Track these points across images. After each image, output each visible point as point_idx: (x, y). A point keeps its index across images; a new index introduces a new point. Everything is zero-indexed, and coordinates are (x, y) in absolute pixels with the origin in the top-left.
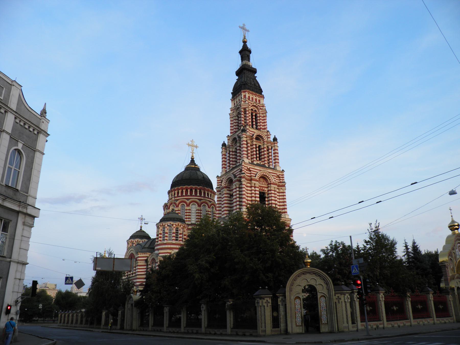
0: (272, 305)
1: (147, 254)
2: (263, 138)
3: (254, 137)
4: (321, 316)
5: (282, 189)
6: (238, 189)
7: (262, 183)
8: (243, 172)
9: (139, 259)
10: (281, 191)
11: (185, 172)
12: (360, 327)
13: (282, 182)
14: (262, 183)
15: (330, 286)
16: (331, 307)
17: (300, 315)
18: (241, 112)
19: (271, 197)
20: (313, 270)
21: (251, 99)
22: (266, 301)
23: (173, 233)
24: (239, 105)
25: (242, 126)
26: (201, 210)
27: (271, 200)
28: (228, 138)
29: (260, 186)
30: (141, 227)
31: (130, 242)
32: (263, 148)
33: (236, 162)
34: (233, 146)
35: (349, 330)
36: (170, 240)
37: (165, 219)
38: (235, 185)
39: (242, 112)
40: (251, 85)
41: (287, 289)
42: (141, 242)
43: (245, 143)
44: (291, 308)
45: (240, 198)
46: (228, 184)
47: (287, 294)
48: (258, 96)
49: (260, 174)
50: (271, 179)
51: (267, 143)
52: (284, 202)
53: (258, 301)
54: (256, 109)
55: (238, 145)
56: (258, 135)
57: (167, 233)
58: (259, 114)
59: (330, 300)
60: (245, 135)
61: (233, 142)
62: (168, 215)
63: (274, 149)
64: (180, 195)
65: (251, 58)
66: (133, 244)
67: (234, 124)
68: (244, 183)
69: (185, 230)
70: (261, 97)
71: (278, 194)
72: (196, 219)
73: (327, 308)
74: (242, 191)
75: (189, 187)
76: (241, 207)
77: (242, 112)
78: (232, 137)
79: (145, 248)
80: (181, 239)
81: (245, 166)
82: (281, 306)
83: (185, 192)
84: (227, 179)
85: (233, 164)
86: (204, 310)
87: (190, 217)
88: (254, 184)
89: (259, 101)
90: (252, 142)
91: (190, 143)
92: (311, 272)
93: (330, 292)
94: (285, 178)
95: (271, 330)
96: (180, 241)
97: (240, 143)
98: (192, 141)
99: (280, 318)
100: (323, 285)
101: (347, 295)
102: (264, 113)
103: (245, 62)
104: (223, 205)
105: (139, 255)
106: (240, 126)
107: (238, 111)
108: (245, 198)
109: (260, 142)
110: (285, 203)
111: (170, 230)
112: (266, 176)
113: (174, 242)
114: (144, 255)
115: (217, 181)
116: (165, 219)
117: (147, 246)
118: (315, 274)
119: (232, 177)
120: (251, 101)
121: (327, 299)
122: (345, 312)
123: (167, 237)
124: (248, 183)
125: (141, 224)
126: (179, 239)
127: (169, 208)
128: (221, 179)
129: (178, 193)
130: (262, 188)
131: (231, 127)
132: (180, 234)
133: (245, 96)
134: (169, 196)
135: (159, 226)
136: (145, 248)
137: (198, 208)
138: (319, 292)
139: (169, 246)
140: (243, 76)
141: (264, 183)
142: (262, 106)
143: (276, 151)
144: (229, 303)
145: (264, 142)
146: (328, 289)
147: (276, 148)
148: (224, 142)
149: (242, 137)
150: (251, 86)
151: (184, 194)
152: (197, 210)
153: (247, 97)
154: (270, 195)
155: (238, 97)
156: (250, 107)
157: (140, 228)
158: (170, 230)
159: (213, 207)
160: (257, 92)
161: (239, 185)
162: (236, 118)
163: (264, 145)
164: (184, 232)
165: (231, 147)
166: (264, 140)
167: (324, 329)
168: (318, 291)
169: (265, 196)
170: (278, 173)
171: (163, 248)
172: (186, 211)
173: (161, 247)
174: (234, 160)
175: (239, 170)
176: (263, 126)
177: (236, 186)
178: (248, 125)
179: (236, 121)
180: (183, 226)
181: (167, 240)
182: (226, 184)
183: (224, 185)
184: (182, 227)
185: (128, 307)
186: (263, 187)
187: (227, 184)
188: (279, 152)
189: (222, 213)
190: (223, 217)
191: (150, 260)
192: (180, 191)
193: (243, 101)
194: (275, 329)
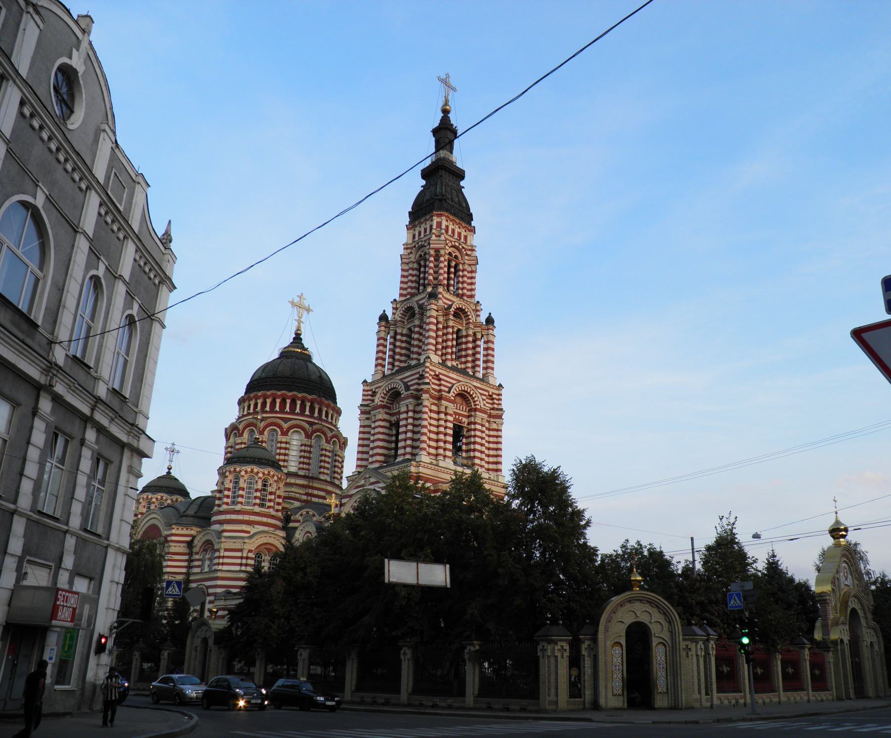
0: (569, 657)
1: (192, 529)
2: (468, 316)
3: (451, 310)
4: (657, 679)
5: (495, 422)
6: (410, 414)
8: (427, 381)
9: (174, 538)
10: (494, 426)
11: (281, 362)
12: (716, 702)
13: (498, 409)
15: (674, 626)
16: (675, 664)
17: (620, 676)
18: (427, 256)
19: (475, 436)
20: (647, 596)
21: (450, 233)
22: (560, 648)
23: (257, 490)
24: (425, 241)
25: (429, 284)
26: (310, 446)
27: (475, 443)
28: (395, 306)
29: (456, 413)
30: (169, 469)
31: (143, 498)
32: (467, 336)
33: (408, 356)
34: (404, 322)
35: (701, 705)
36: (248, 504)
37: (241, 459)
38: (405, 405)
39: (431, 256)
40: (453, 204)
41: (601, 628)
42: (169, 501)
43: (435, 321)
44: (606, 662)
45: (414, 432)
46: (388, 401)
47: (601, 636)
48: (463, 228)
49: (458, 388)
50: (477, 401)
51: (475, 327)
52: (497, 449)
53: (543, 646)
54: (458, 254)
55: (417, 322)
56: (458, 309)
57: (243, 489)
59: (674, 652)
60: (435, 305)
61: (406, 316)
62: (247, 451)
63: (486, 340)
64: (268, 409)
65: (455, 147)
66: (150, 503)
67: (410, 278)
68: (426, 403)
69: (281, 485)
70: (470, 231)
71: (487, 432)
72: (298, 463)
73: (668, 665)
74: (420, 419)
75: (290, 394)
76: (415, 451)
77: (431, 256)
78: (404, 304)
79: (187, 516)
80: (272, 504)
81: (431, 370)
82: (586, 658)
83: (280, 403)
84: (387, 390)
85: (401, 361)
86: (408, 659)
87: (286, 458)
88: (444, 407)
89: (466, 237)
90: (447, 320)
91: (297, 300)
92: (644, 599)
93: (674, 637)
94: (502, 402)
95: (567, 701)
96: (269, 507)
97: (421, 320)
98: (300, 297)
99: (584, 681)
100: (663, 623)
101: (701, 643)
102: (473, 265)
103: (443, 153)
104: (373, 441)
105: (174, 531)
106: (425, 286)
107: (419, 253)
108: (425, 434)
109: (460, 323)
110: (499, 453)
111: (250, 483)
112: (469, 393)
113: (257, 509)
114: (185, 532)
115: (364, 390)
116: (241, 457)
117: (191, 512)
118: (650, 603)
119: (401, 389)
120: (450, 236)
121: (668, 648)
122: (696, 673)
123: (242, 496)
125: (171, 461)
126: (268, 504)
127: (241, 435)
128: (373, 387)
129: (264, 404)
130: (457, 417)
131: (402, 282)
132: (271, 493)
133: (439, 225)
134: (241, 409)
135: (226, 472)
136: (187, 516)
137: (306, 441)
138: (656, 635)
139: (246, 517)
140: (439, 182)
142: (469, 250)
143: (490, 345)
144: (472, 649)
145: (469, 323)
146: (671, 632)
147: (491, 338)
148: (384, 311)
149: (428, 308)
150: (453, 206)
151: (277, 408)
152: (302, 445)
153: (443, 227)
154: (473, 433)
155: (424, 223)
156: (447, 247)
157: (167, 470)
158: (250, 483)
159: (334, 441)
160: (462, 219)
161: (415, 406)
162: (416, 266)
163: (467, 329)
164: (279, 489)
165: (399, 324)
166: (469, 319)
167: (660, 701)
168: (653, 634)
169: (461, 434)
170: (491, 391)
171: (233, 520)
172: (279, 445)
173: (228, 517)
174: (403, 352)
175: (417, 376)
176: (468, 290)
177: (408, 408)
178: (441, 285)
179: (415, 272)
180: (278, 477)
181: (241, 503)
182: (384, 400)
183: (380, 401)
184: (276, 478)
185: (192, 643)
186: (460, 415)
187: (385, 400)
188: (495, 346)
189: (371, 460)
190: (370, 466)
191: (200, 544)
192: (269, 401)
193: (434, 233)
194: (573, 699)
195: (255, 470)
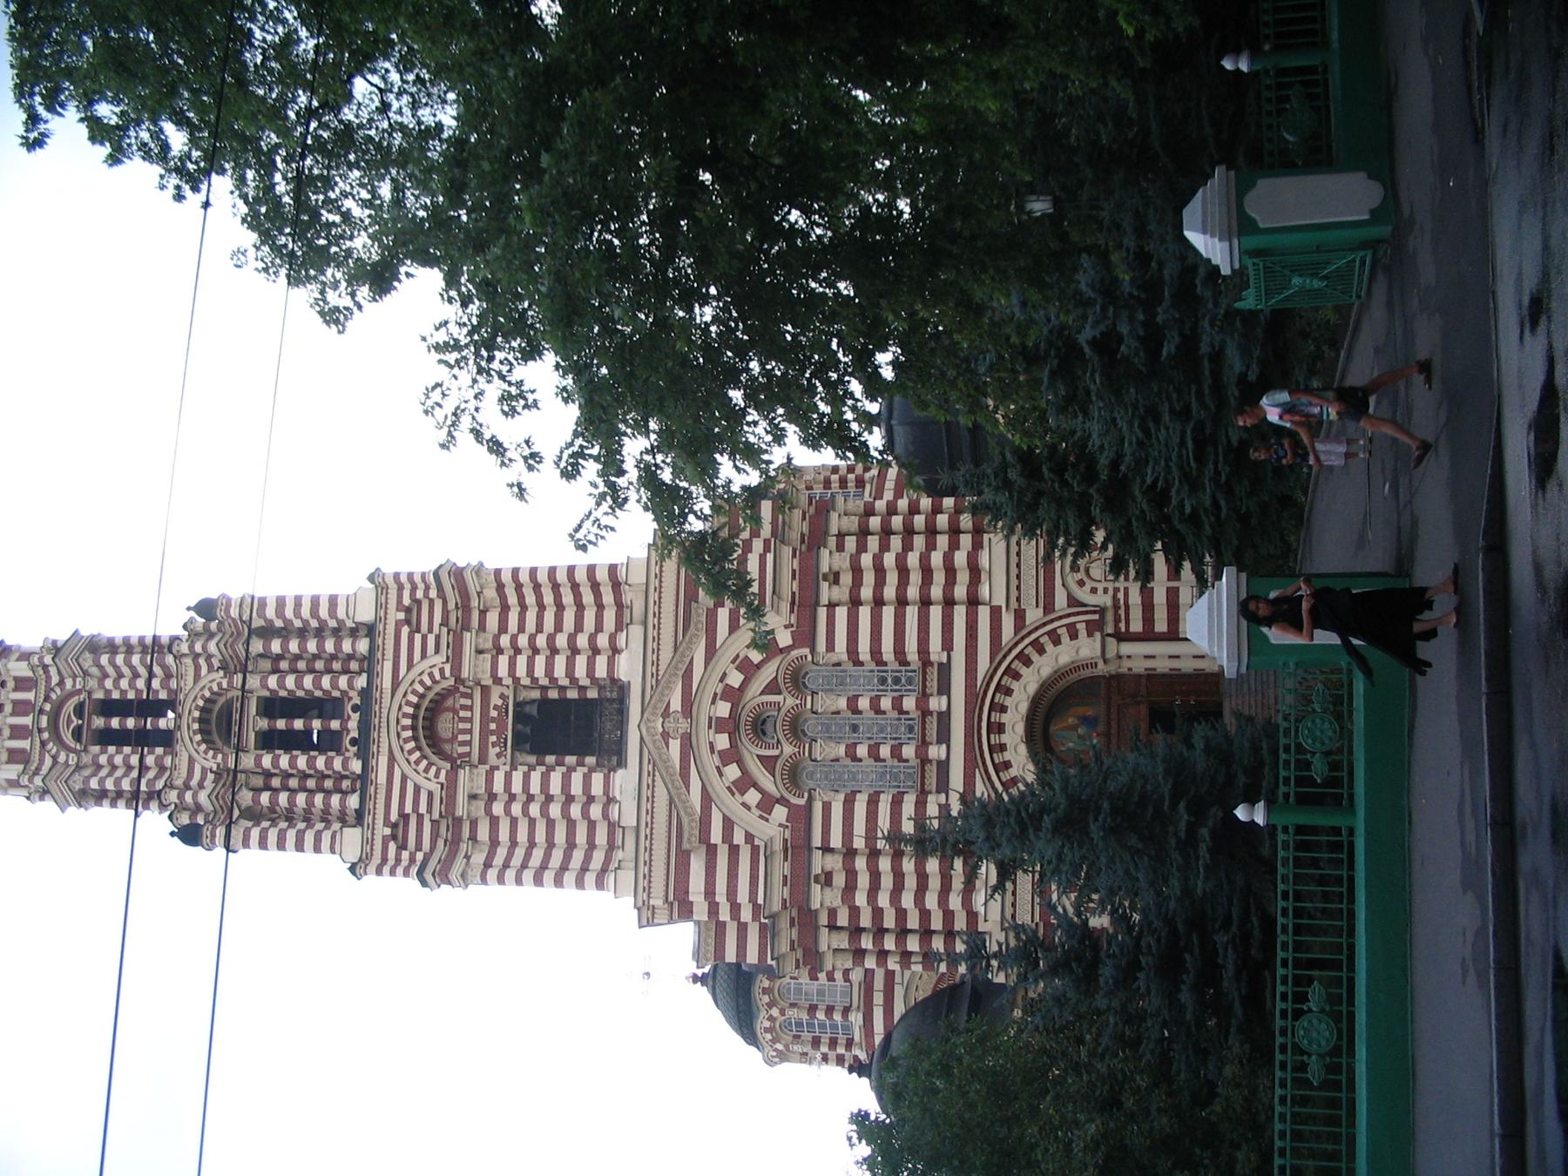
7: (461, 726)
10: (491, 593)
14: (461, 726)
50: (431, 675)
58: (90, 693)
124: (473, 838)
141: (464, 707)
154: (526, 681)
195: (767, 1024)
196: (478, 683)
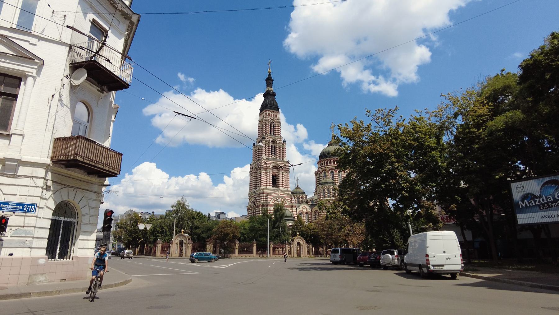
32: (277, 148)
54: (274, 122)
70: (278, 113)
89: (276, 116)
133: (266, 114)
153: (268, 115)
176: (277, 133)
196: (279, 172)
